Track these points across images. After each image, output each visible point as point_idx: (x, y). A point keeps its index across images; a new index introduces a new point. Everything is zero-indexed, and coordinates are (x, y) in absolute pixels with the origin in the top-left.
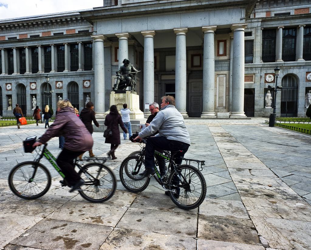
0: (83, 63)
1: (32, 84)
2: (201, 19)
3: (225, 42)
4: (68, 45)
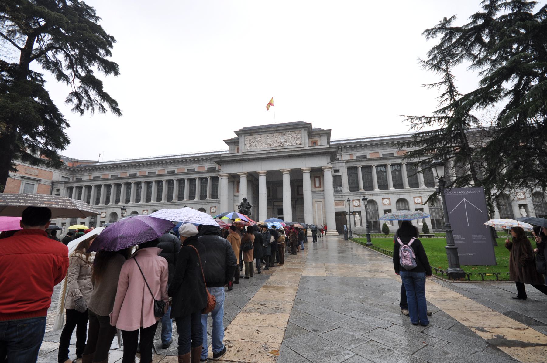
0: (211, 193)
3: (319, 177)
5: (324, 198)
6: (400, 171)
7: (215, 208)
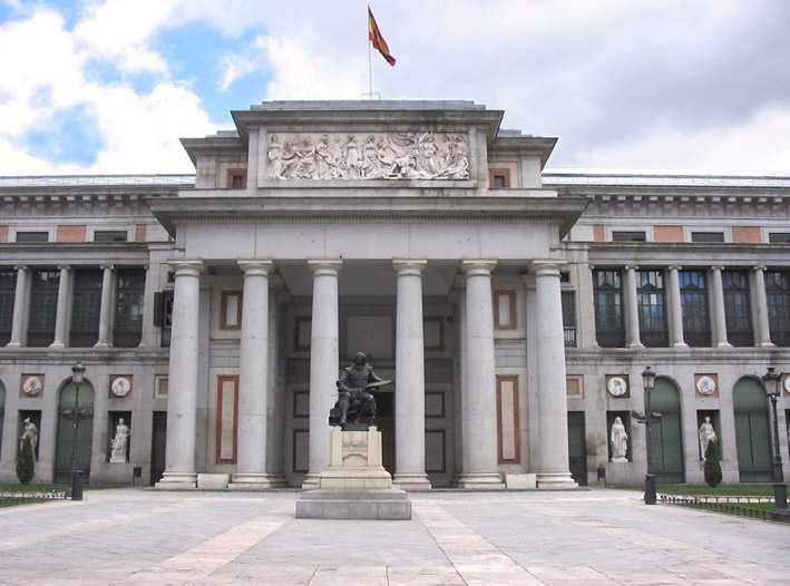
2: (460, 242)
3: (512, 295)
4: (69, 271)
5: (526, 366)
6: (705, 292)
7: (126, 382)
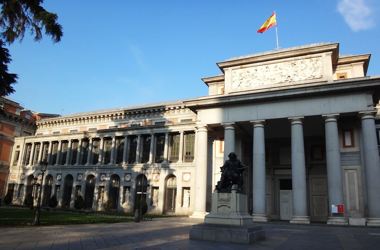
1: (127, 175)
